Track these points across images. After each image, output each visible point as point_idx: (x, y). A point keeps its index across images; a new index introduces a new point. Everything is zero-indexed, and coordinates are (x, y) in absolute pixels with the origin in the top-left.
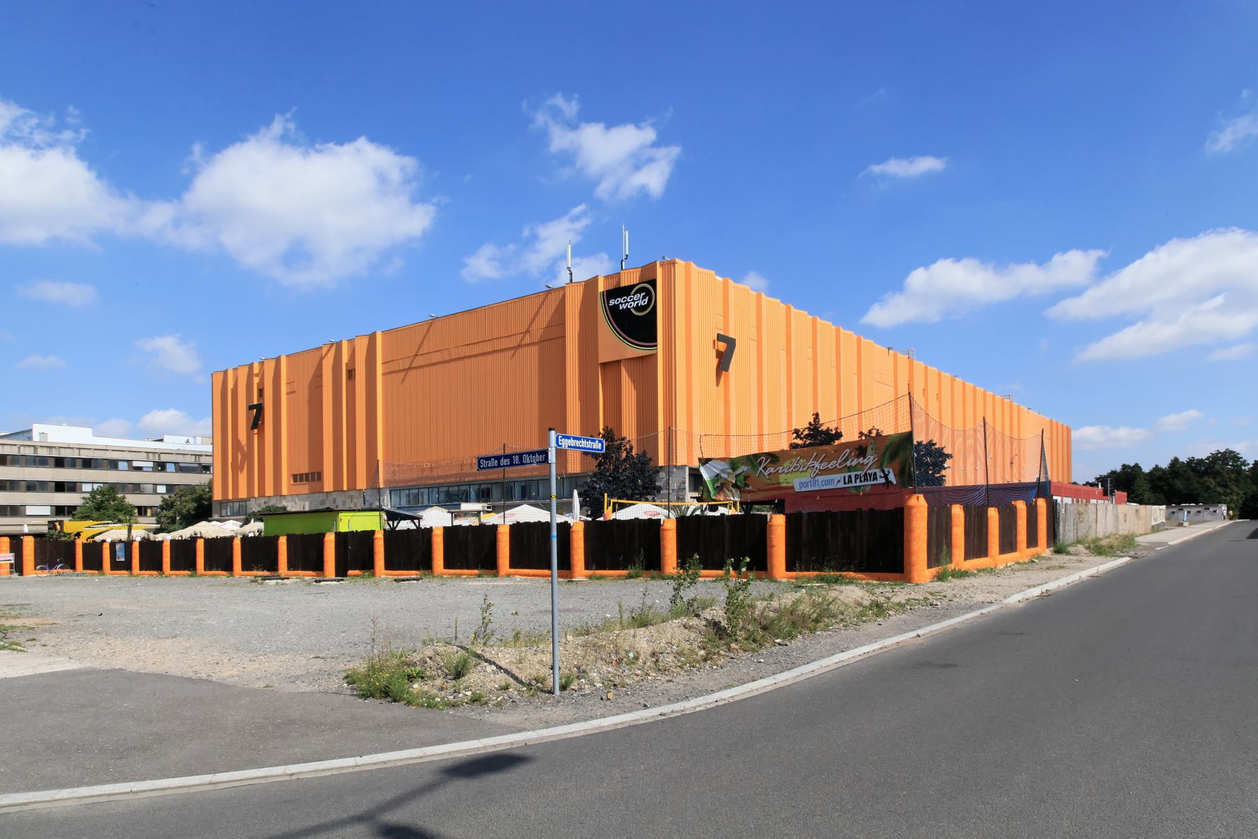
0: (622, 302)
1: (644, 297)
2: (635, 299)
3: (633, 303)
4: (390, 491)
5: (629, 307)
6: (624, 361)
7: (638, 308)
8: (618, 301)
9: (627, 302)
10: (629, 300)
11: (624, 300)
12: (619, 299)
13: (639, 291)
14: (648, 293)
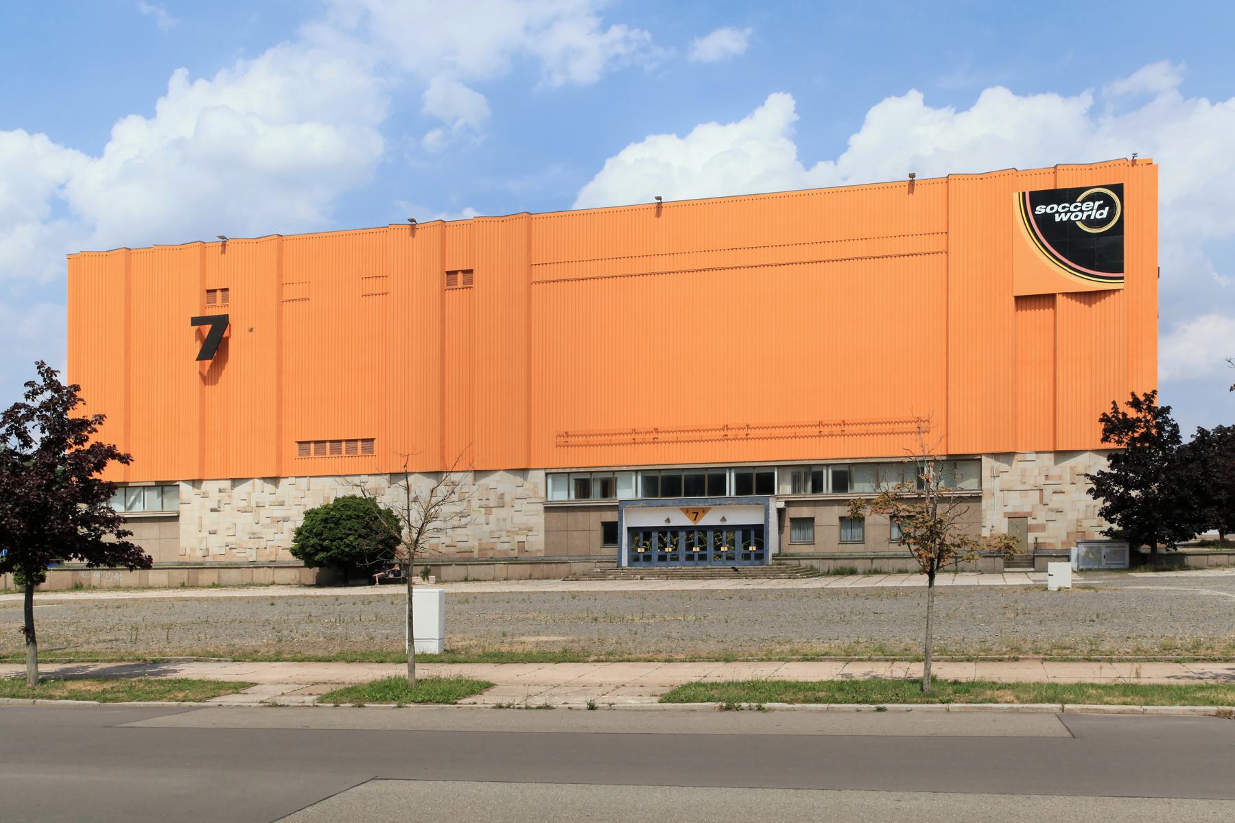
0: (1060, 210)
1: (1101, 207)
2: (1084, 208)
3: (1080, 214)
4: (547, 474)
5: (1073, 218)
6: (1061, 296)
7: (1089, 222)
8: (1052, 209)
9: (1069, 211)
10: (1072, 209)
11: (1064, 208)
12: (1055, 206)
13: (1092, 198)
14: (1108, 202)
